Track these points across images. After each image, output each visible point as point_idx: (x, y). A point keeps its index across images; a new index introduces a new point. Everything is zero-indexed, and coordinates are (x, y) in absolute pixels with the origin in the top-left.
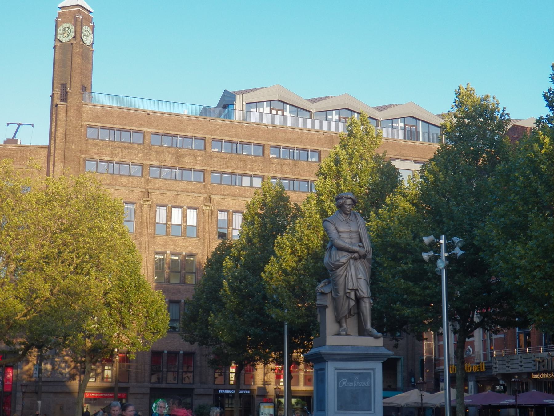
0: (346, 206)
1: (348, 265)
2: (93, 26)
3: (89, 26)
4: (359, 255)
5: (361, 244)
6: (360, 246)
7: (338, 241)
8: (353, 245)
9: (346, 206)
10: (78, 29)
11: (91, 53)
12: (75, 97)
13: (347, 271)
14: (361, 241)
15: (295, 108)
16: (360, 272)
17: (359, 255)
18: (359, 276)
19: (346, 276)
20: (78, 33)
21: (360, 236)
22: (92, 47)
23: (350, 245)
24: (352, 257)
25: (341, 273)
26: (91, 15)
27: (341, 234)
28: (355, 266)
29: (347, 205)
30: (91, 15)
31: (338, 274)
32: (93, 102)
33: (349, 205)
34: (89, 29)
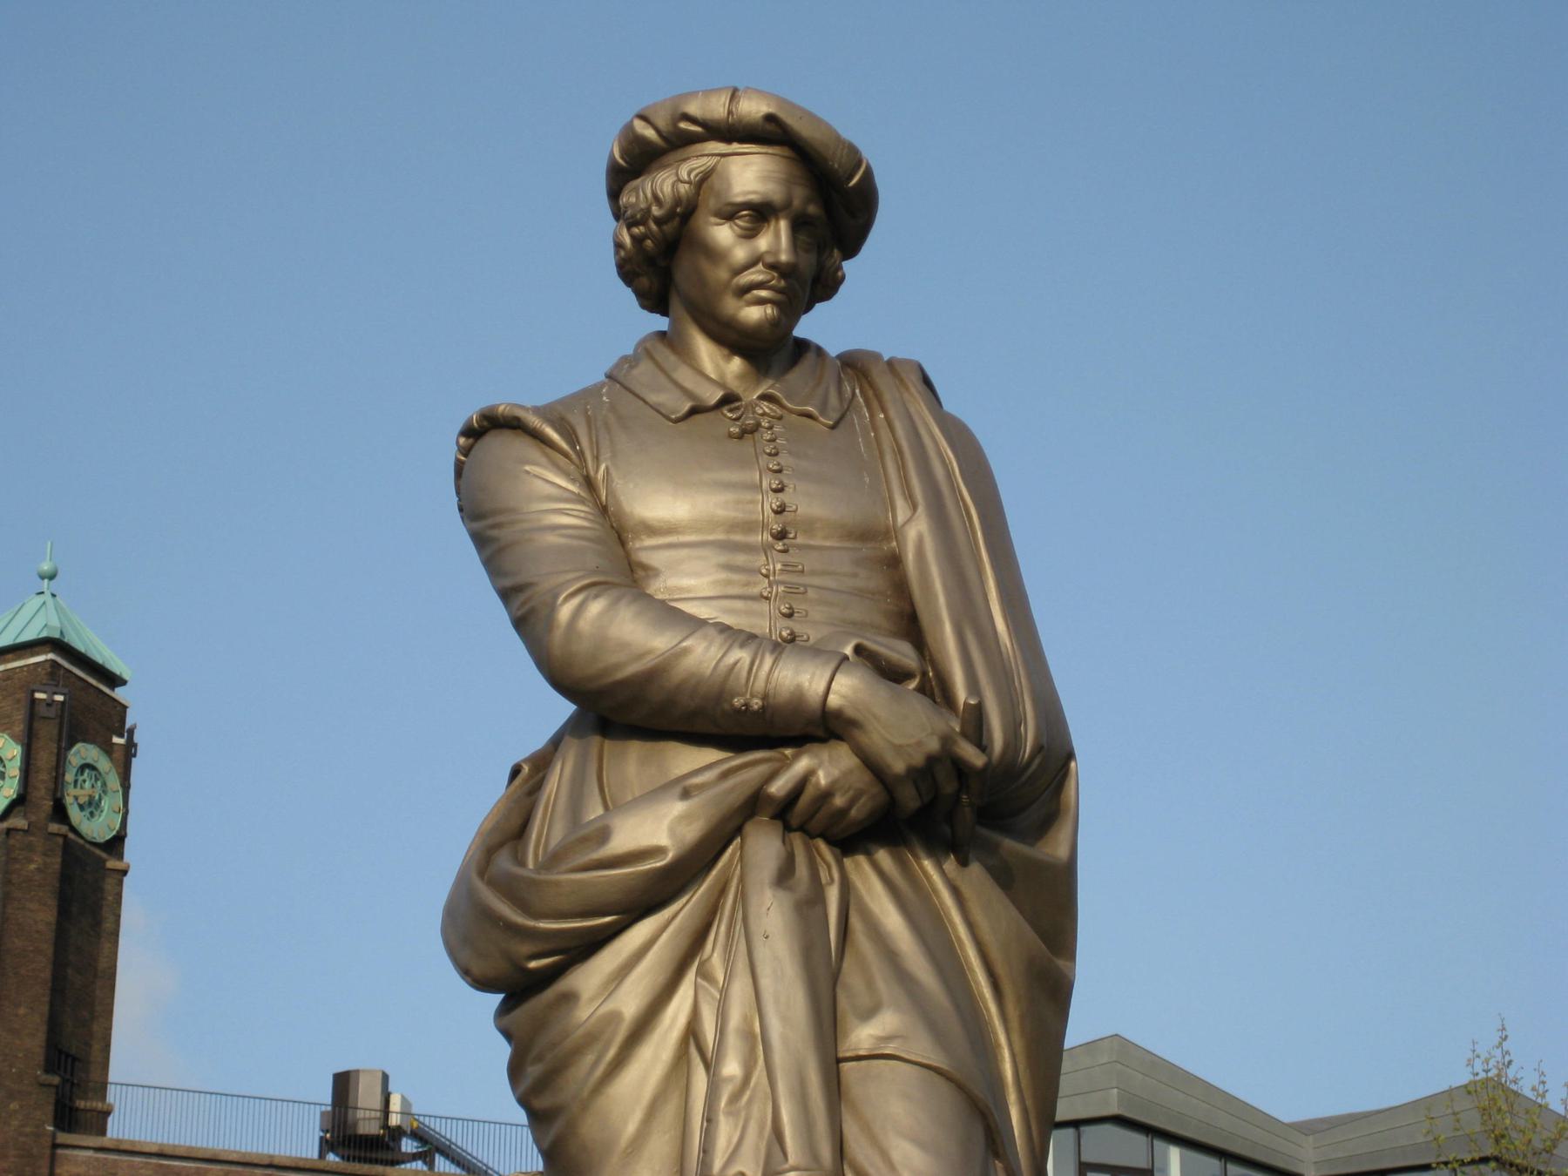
0: (723, 234)
1: (722, 891)
2: (130, 750)
3: (108, 749)
4: (871, 765)
5: (902, 653)
6: (892, 674)
7: (596, 607)
8: (787, 644)
9: (723, 234)
10: (45, 759)
11: (109, 884)
12: (14, 1106)
13: (704, 973)
14: (911, 626)
15: (1213, 1163)
16: (884, 985)
17: (871, 765)
18: (863, 1036)
19: (692, 1032)
20: (43, 778)
21: (901, 588)
22: (120, 856)
23: (732, 635)
24: (778, 787)
25: (629, 1001)
26: (119, 694)
27: (646, 550)
28: (809, 907)
29: (729, 214)
30: (119, 694)
31: (584, 1013)
32: (117, 1129)
33: (760, 214)
34: (104, 764)
